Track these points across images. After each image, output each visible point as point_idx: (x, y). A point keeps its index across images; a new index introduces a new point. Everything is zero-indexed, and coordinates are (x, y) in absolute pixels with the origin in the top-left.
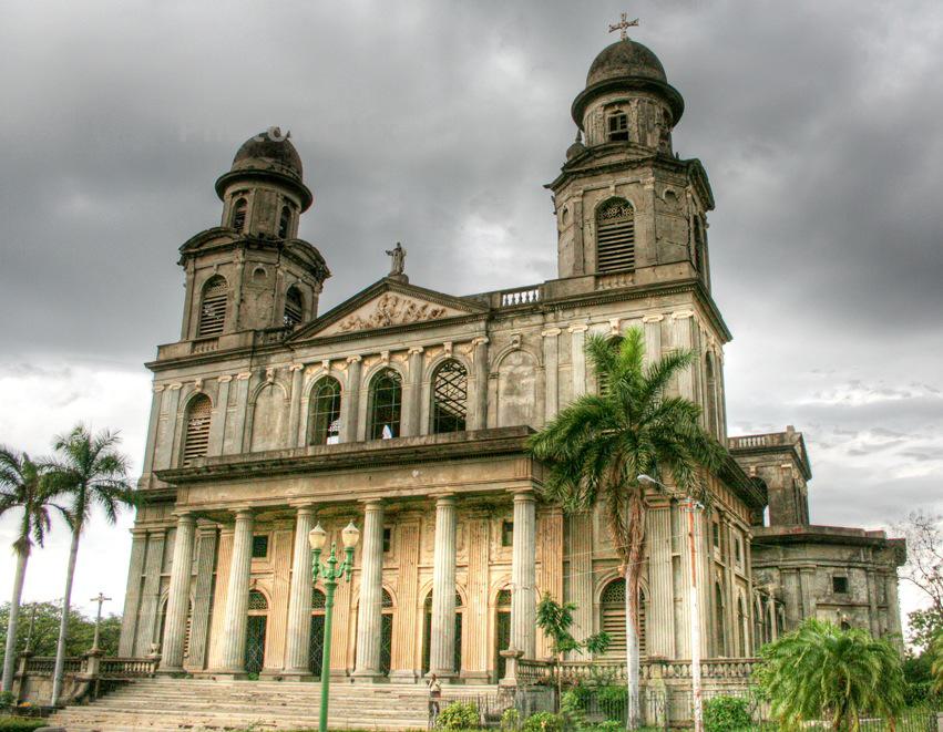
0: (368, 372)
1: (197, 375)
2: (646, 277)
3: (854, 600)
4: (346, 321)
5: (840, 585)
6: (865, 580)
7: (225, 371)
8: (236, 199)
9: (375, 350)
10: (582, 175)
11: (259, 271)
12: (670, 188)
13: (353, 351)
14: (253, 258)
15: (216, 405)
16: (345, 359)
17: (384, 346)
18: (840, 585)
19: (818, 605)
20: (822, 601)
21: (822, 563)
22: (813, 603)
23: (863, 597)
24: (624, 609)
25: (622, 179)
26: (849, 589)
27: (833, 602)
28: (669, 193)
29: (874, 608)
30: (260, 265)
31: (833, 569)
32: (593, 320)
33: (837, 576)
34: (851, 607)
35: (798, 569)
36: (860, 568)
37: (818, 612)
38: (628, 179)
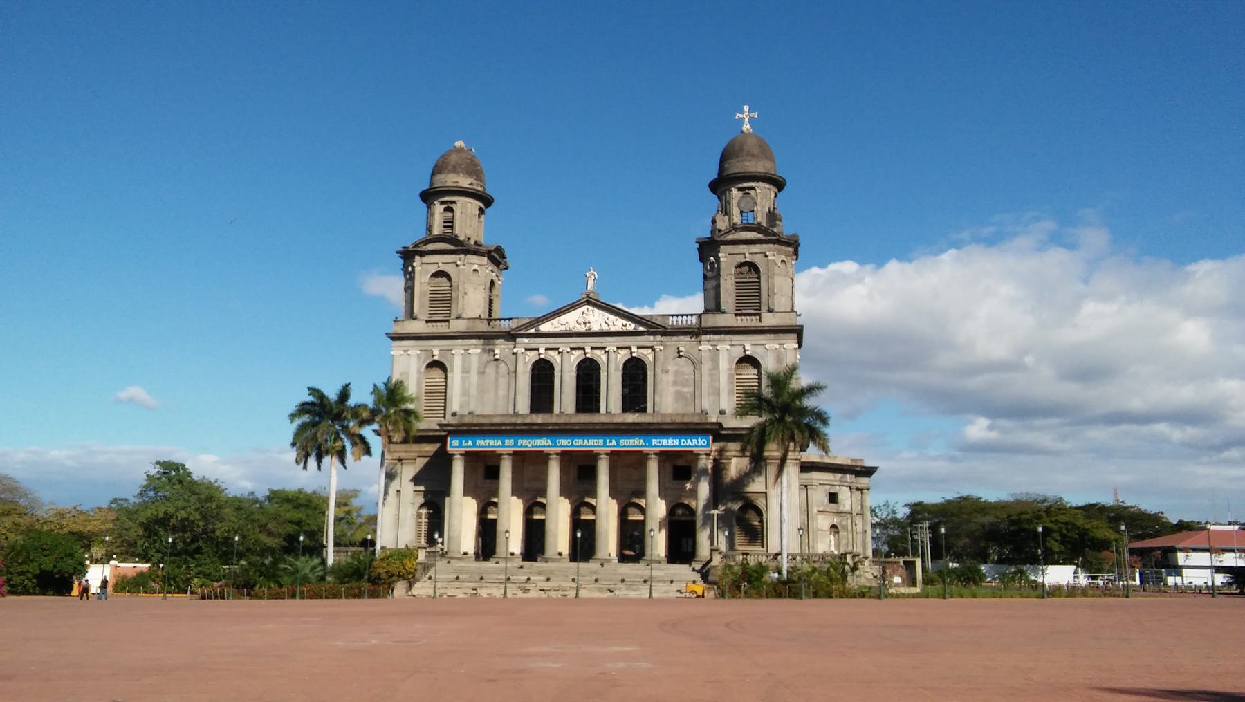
0: (574, 360)
1: (436, 349)
2: (768, 320)
3: (841, 508)
4: (555, 321)
5: (833, 498)
6: (849, 494)
7: (458, 347)
8: (445, 206)
9: (581, 345)
11: (475, 270)
12: (783, 258)
13: (564, 344)
14: (472, 261)
15: (452, 371)
16: (557, 349)
17: (588, 342)
18: (833, 498)
19: (818, 511)
20: (821, 509)
21: (821, 482)
22: (815, 511)
23: (847, 508)
24: (713, 515)
26: (839, 501)
27: (828, 510)
28: (782, 261)
29: (854, 514)
30: (476, 267)
31: (829, 487)
32: (733, 343)
33: (832, 491)
34: (839, 513)
35: (806, 486)
36: (847, 486)
37: (818, 516)
38: (758, 251)
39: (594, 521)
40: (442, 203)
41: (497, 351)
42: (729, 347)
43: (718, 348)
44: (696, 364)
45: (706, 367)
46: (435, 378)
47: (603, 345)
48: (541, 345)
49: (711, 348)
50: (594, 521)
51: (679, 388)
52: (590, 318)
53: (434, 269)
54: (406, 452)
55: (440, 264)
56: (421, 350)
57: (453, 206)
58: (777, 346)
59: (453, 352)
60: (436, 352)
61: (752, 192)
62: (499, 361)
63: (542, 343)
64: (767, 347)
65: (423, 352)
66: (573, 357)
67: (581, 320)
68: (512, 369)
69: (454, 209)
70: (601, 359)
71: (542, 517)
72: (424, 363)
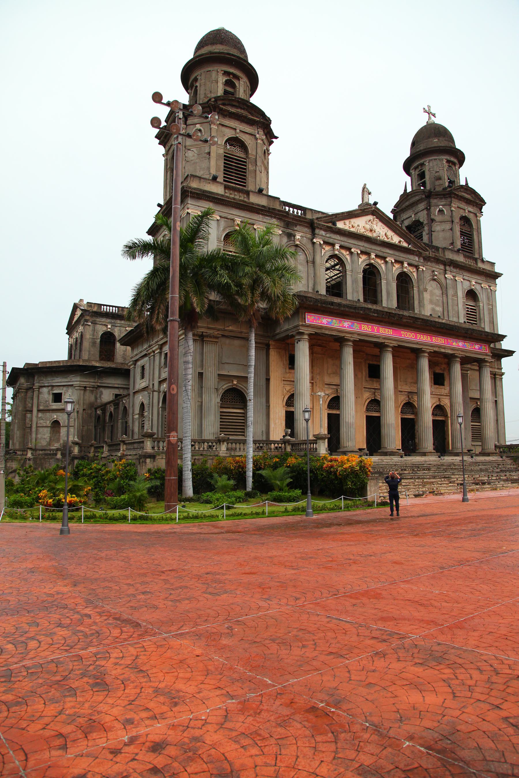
0: (362, 262)
10: (456, 197)
25: (471, 209)
39: (379, 418)
40: (226, 73)
41: (298, 237)
42: (462, 280)
43: (456, 278)
44: (444, 289)
45: (450, 292)
46: (231, 252)
47: (385, 255)
48: (336, 241)
49: (452, 278)
50: (379, 418)
51: (433, 306)
52: (375, 227)
53: (230, 134)
54: (208, 328)
55: (238, 131)
56: (220, 217)
57: (236, 82)
58: (488, 287)
59: (255, 227)
60: (238, 221)
61: (453, 166)
62: (298, 248)
63: (338, 240)
64: (482, 285)
65: (223, 219)
66: (360, 260)
67: (368, 227)
68: (310, 259)
69: (237, 85)
70: (381, 267)
71: (338, 412)
72: (224, 230)
